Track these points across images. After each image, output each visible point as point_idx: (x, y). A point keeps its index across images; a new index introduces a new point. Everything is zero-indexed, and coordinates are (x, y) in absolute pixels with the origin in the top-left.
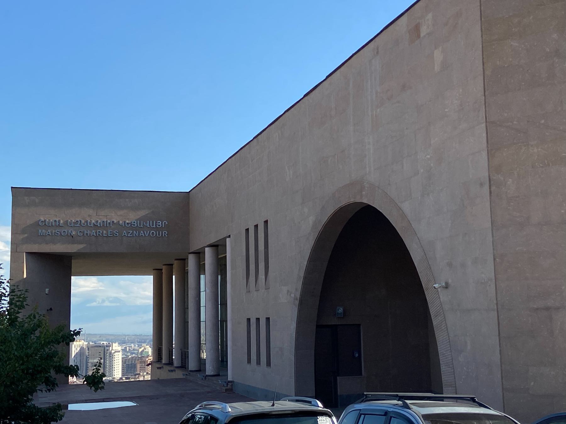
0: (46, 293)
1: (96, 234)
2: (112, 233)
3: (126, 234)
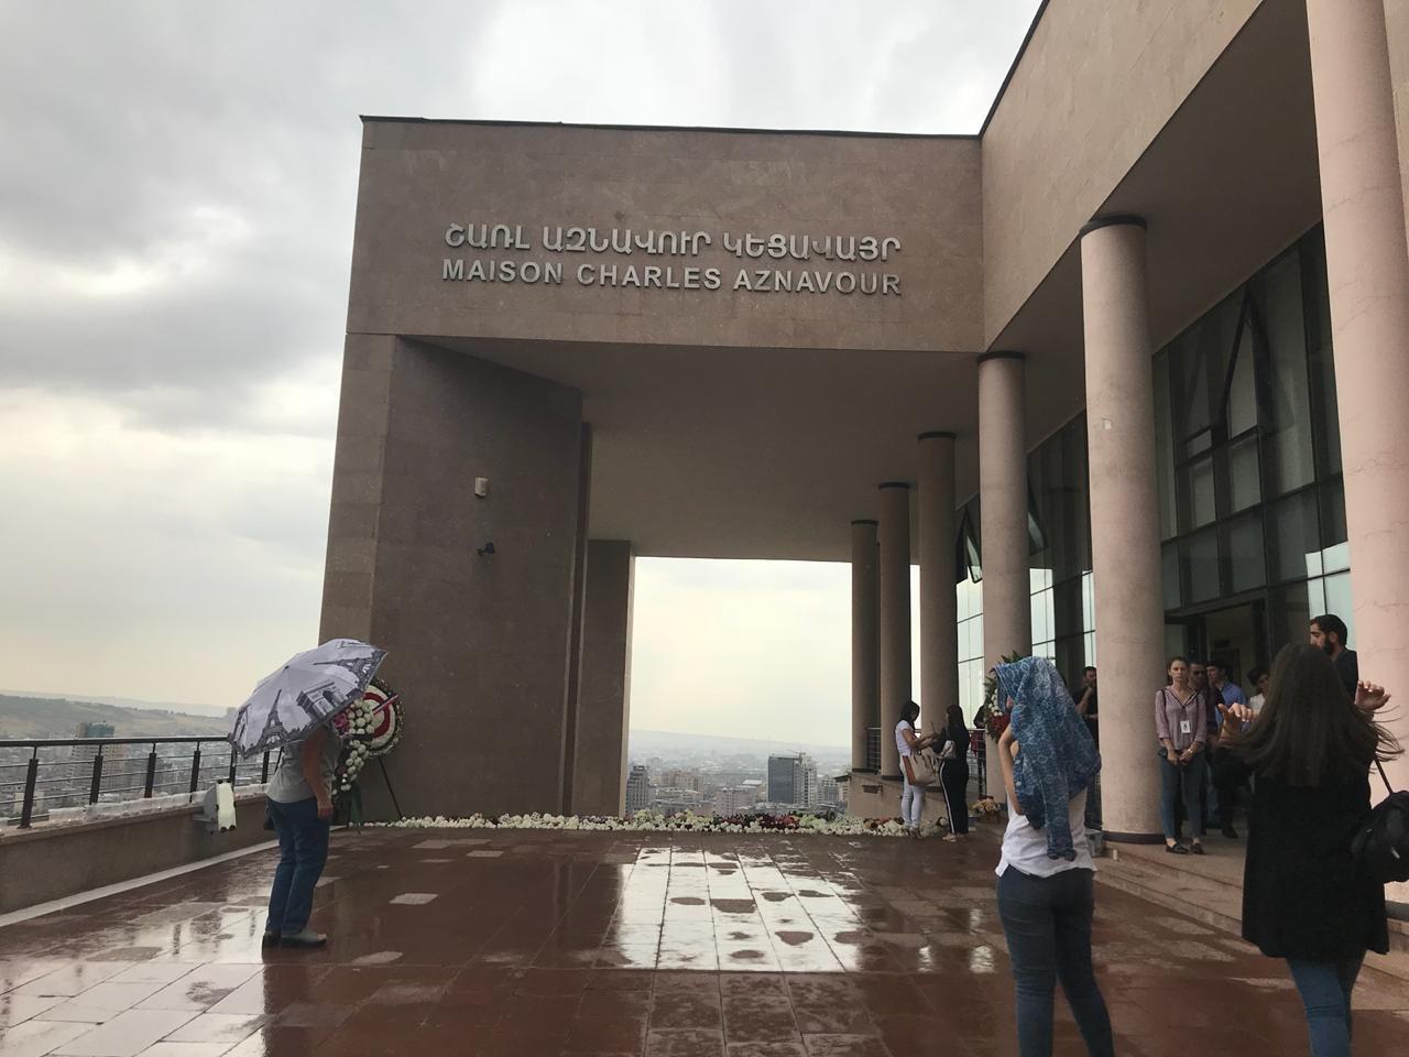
0: (477, 492)
1: (643, 281)
2: (696, 277)
3: (747, 283)
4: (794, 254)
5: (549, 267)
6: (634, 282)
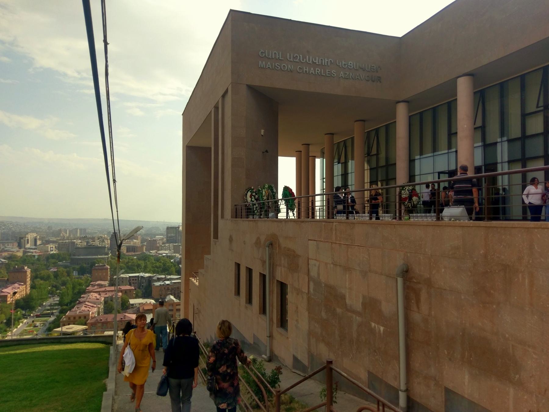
0: (262, 134)
1: (315, 73)
3: (343, 75)
4: (355, 68)
5: (289, 67)
6: (342, 77)
